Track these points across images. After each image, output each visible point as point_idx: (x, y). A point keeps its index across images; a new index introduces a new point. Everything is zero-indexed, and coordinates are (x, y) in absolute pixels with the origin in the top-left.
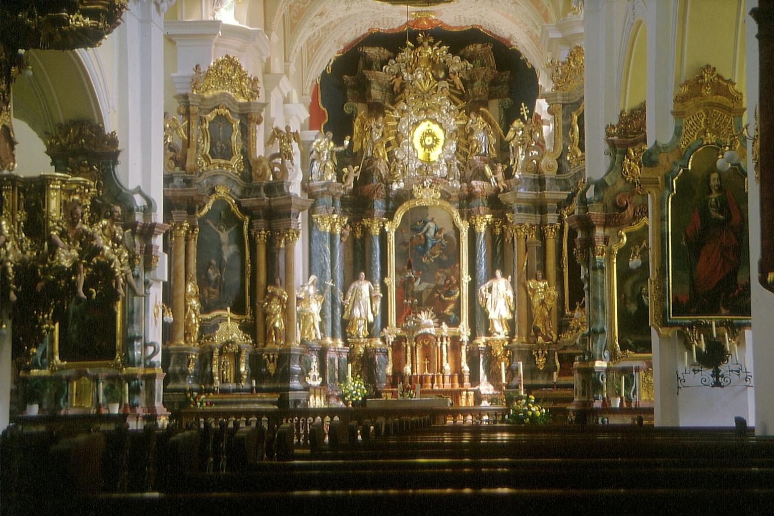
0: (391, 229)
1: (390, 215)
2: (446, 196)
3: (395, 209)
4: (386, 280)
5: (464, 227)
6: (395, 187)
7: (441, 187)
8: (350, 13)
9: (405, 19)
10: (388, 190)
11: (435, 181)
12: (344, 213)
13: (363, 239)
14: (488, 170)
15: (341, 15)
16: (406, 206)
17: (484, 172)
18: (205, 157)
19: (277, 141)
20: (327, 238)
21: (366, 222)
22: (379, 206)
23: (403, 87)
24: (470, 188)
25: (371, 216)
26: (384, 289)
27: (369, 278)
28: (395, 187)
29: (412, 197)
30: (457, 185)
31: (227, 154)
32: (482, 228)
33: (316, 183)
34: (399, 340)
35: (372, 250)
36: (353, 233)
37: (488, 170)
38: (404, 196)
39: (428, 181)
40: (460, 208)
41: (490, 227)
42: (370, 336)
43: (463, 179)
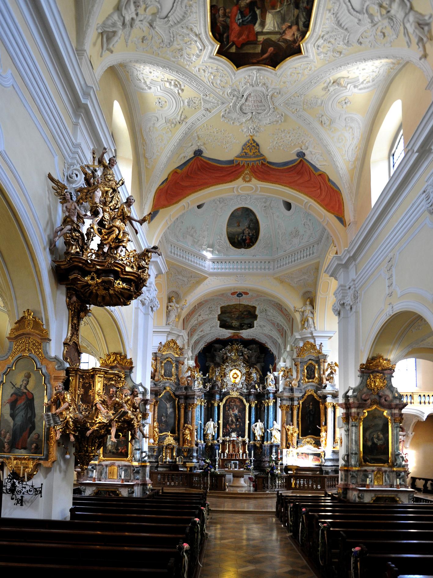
0: (221, 405)
1: (221, 400)
2: (241, 394)
3: (223, 398)
4: (220, 422)
5: (247, 405)
6: (223, 390)
7: (239, 391)
8: (212, 331)
9: (230, 335)
10: (221, 391)
11: (237, 389)
12: (205, 399)
13: (211, 408)
14: (256, 386)
15: (208, 332)
16: (227, 397)
17: (255, 386)
18: (162, 376)
19: (190, 372)
20: (199, 406)
21: (213, 402)
22: (217, 397)
23: (227, 358)
24: (250, 392)
25: (215, 400)
26: (219, 424)
27: (213, 421)
28: (223, 390)
29: (229, 394)
30: (245, 391)
31: (171, 375)
32: (253, 405)
33: (196, 388)
34: (224, 441)
35: (214, 411)
36: (208, 405)
37: (256, 386)
38: (227, 393)
39: (235, 389)
40: (246, 399)
41: (256, 405)
42: (213, 440)
43: (247, 389)
